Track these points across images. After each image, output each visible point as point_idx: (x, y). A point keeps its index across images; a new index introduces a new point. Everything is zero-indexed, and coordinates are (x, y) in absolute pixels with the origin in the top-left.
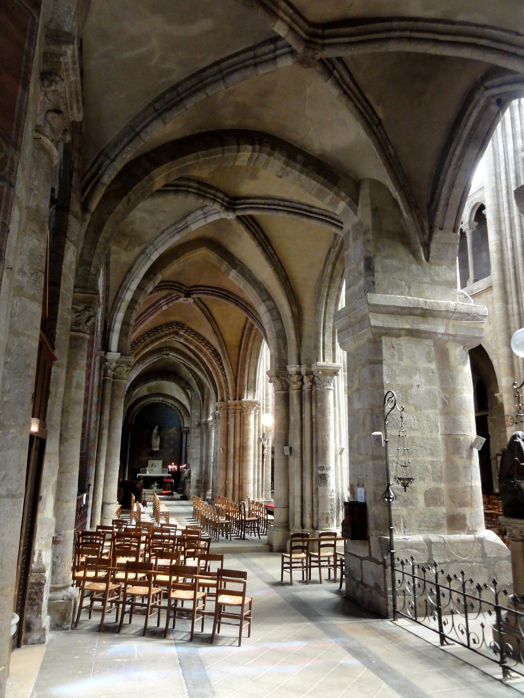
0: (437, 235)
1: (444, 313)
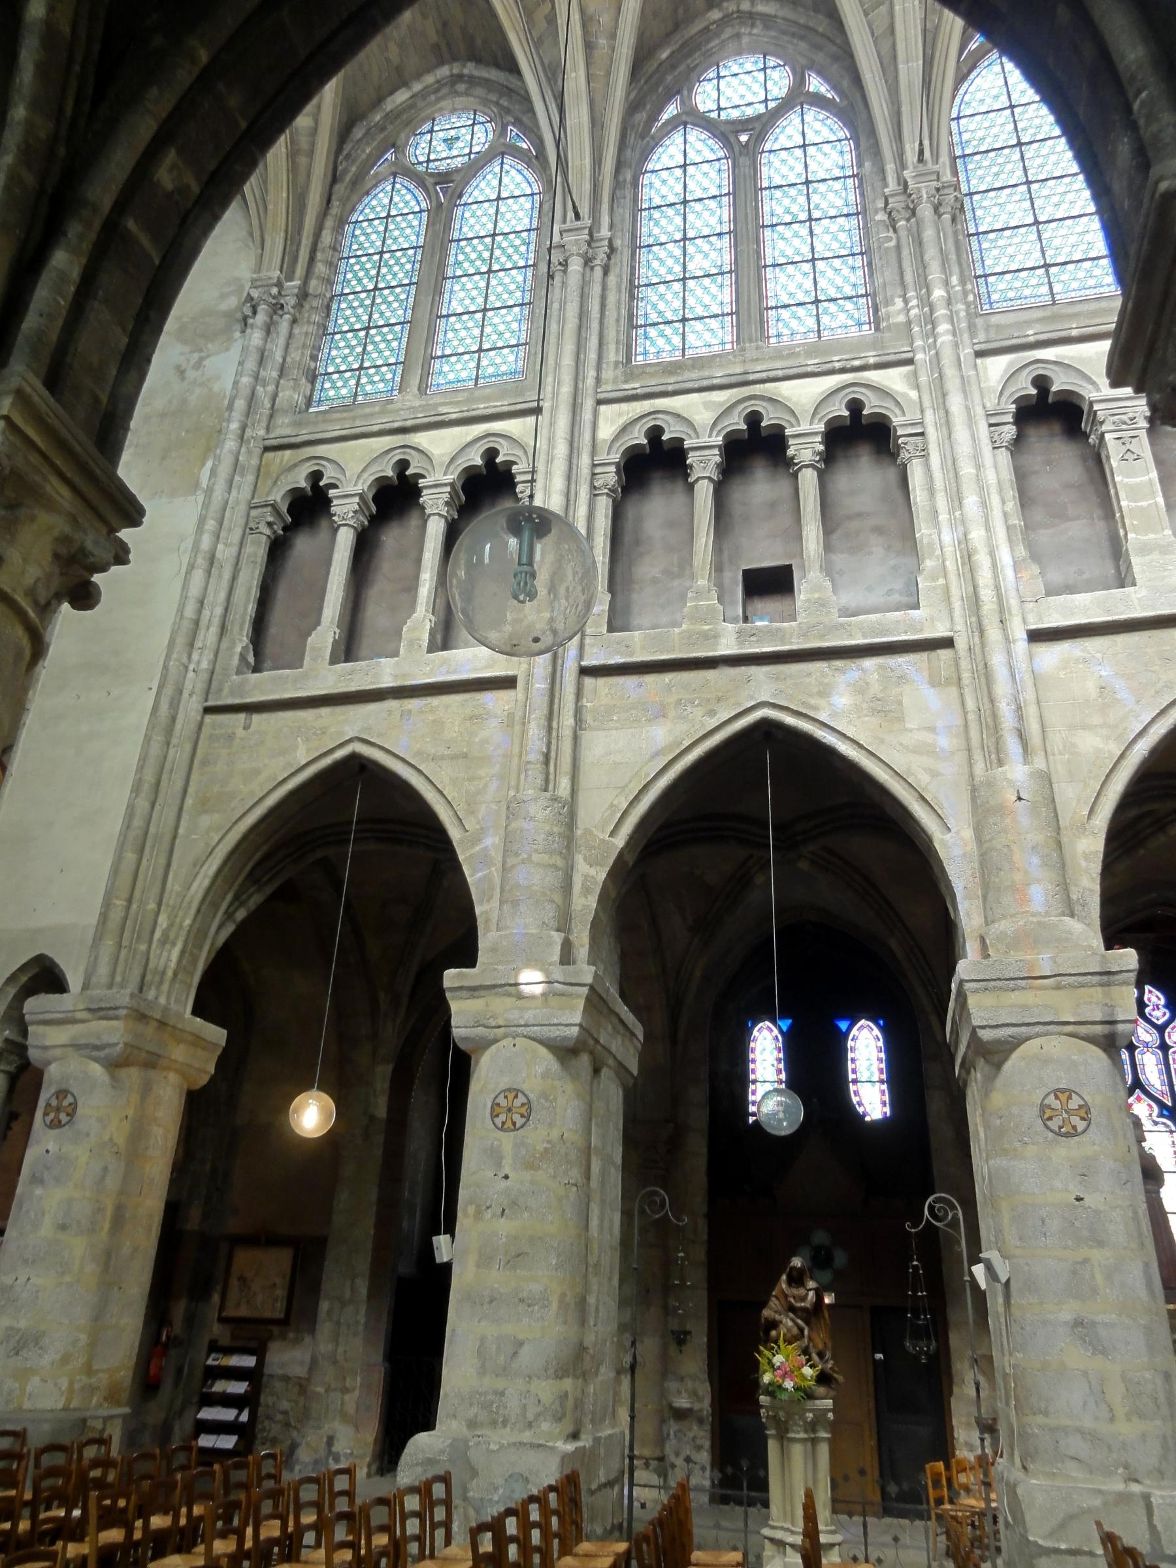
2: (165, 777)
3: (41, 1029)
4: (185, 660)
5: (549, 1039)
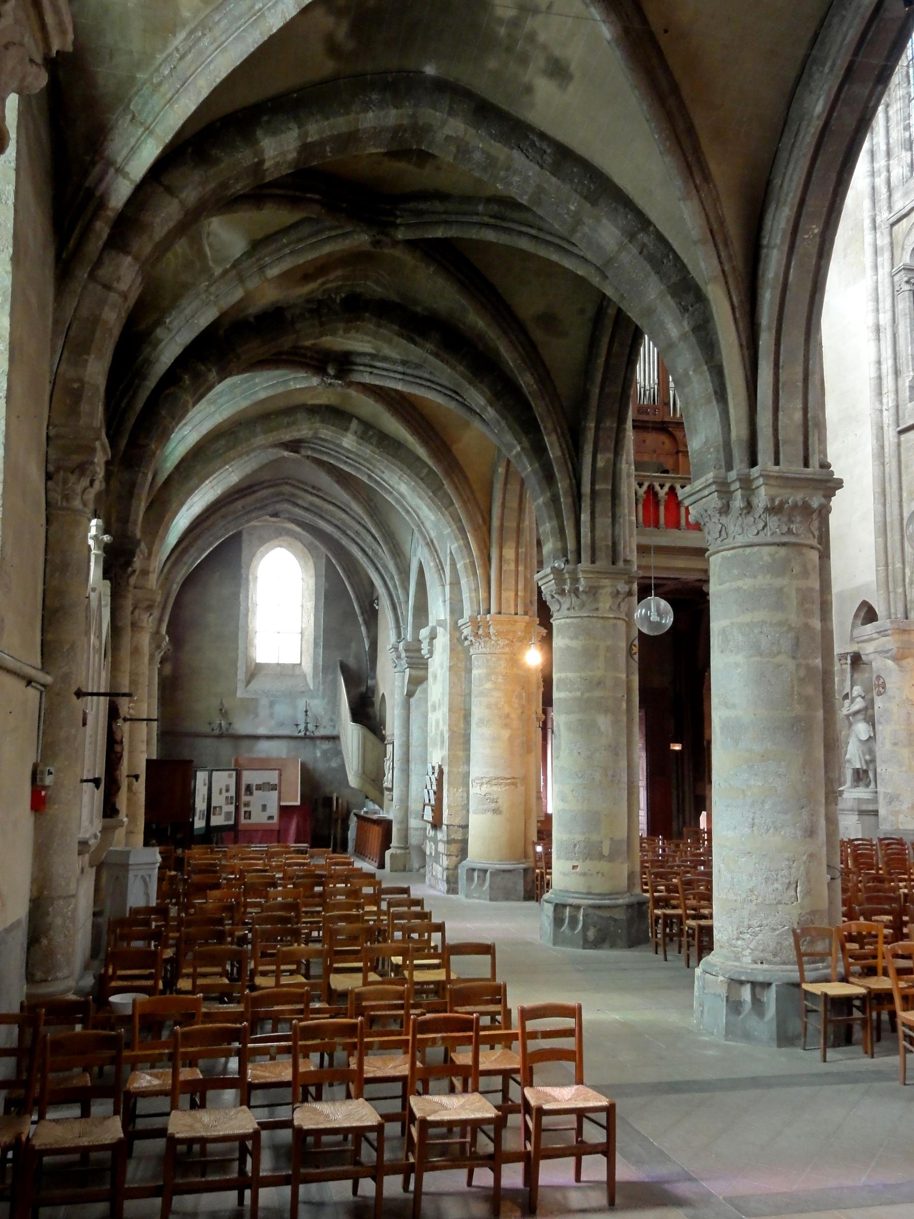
2: (887, 485)
4: (878, 406)
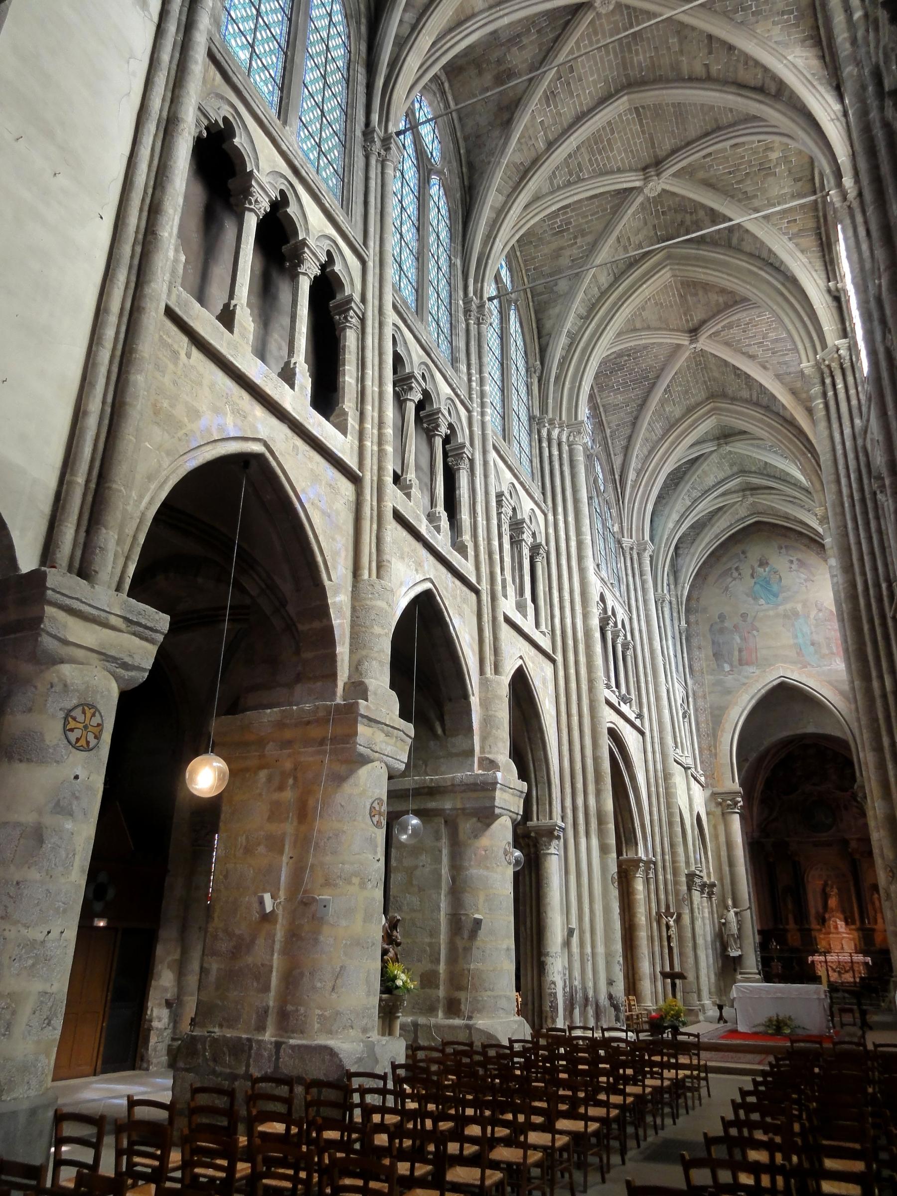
0: (448, 707)
1: (450, 788)
3: (61, 615)
5: (393, 768)
